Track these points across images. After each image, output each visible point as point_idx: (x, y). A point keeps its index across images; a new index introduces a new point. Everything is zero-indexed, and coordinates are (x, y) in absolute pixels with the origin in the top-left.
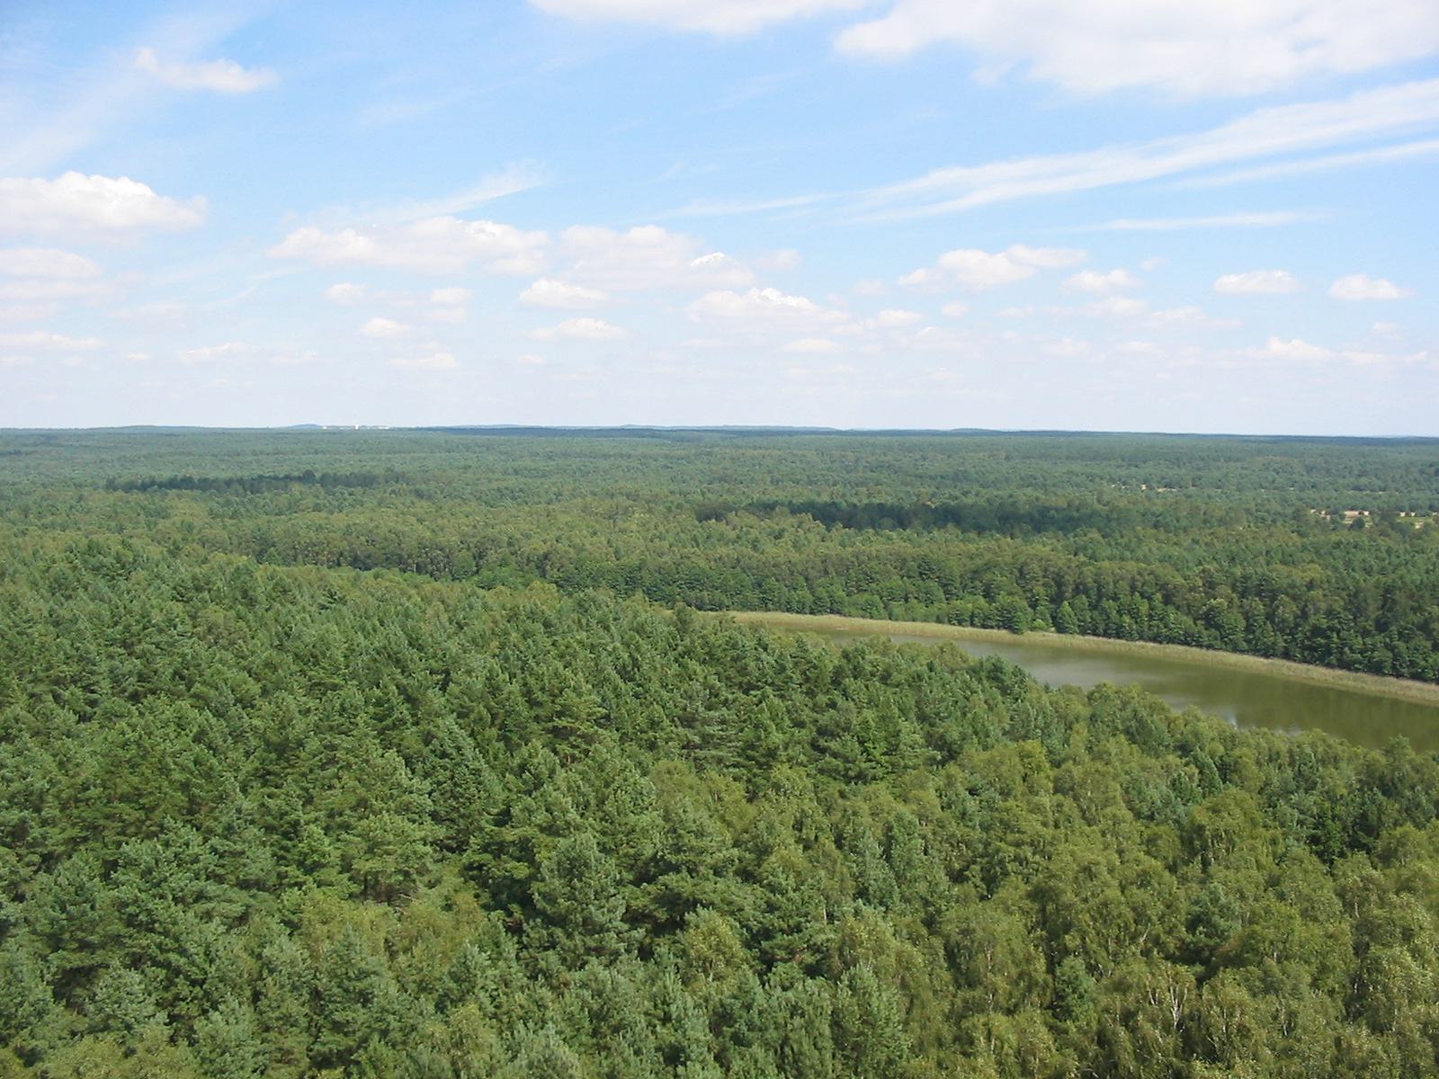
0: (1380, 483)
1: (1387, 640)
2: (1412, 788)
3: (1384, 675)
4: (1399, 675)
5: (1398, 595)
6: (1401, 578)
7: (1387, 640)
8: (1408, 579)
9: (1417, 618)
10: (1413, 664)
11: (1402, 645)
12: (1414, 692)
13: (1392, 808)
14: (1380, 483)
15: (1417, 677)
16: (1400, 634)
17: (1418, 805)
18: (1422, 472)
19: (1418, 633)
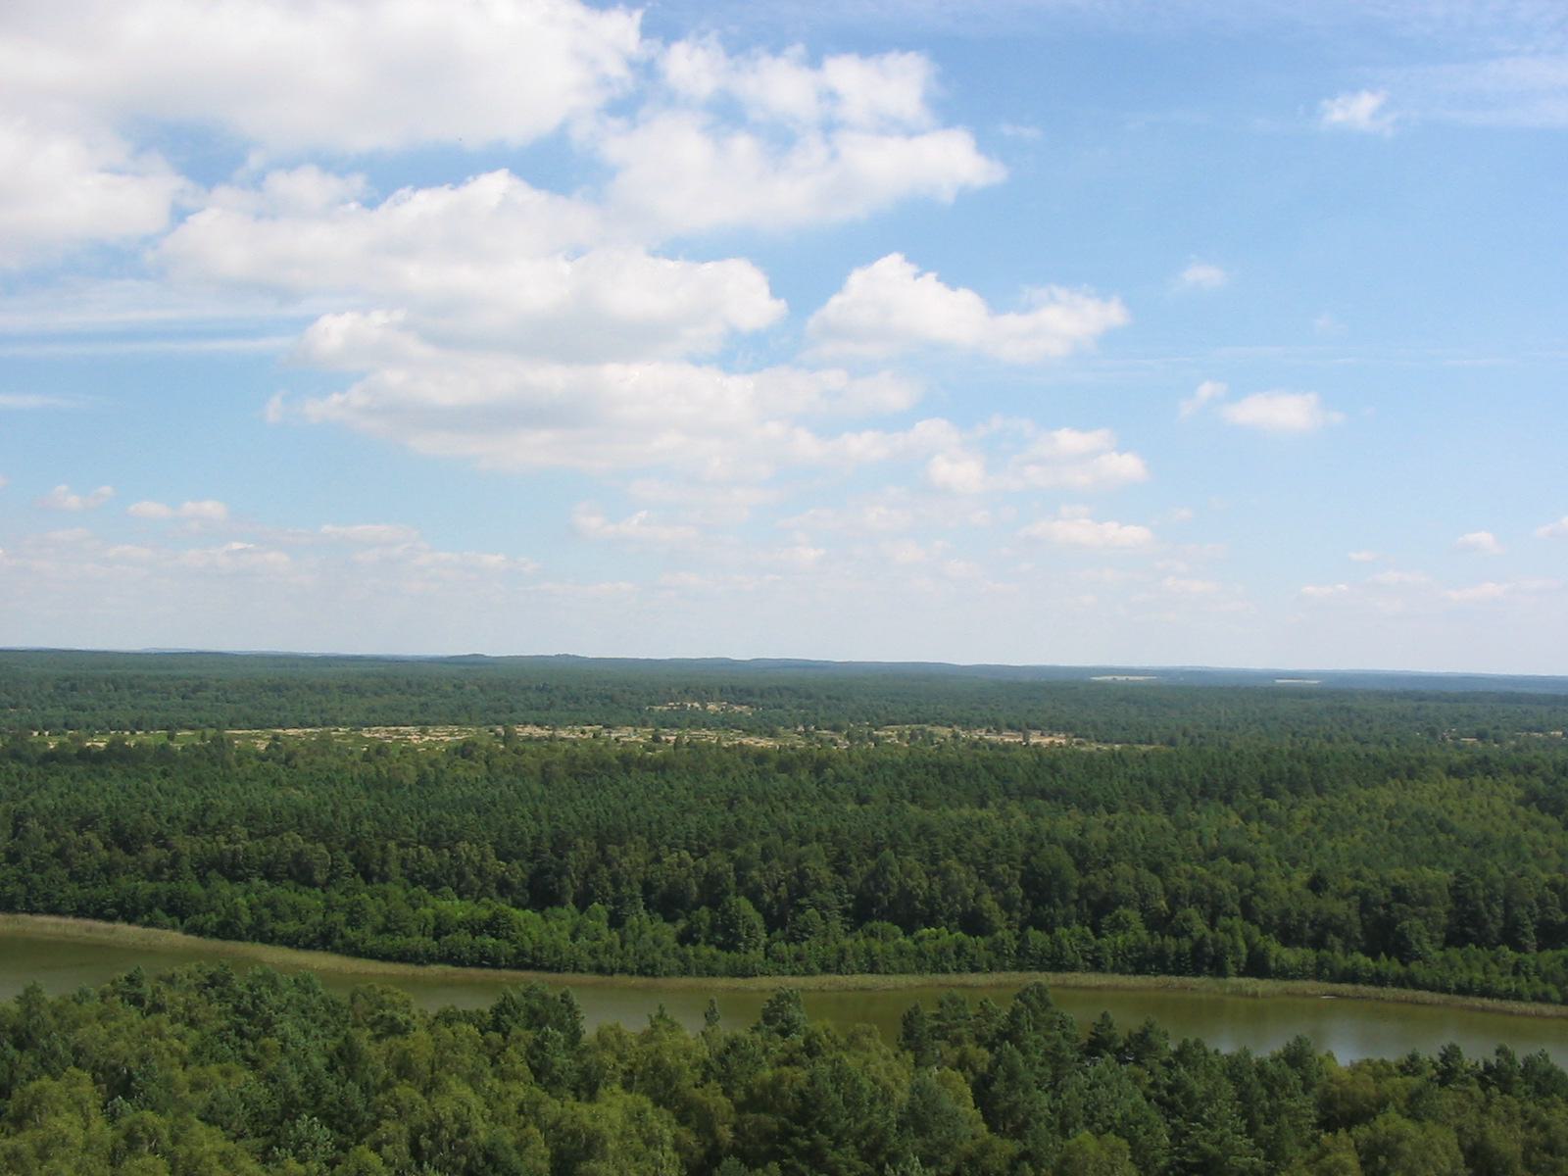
0: (9, 699)
1: (20, 873)
2: (48, 1036)
3: (17, 912)
4: (33, 912)
5: (32, 824)
6: (32, 804)
7: (20, 873)
8: (40, 805)
9: (52, 846)
10: (47, 897)
11: (36, 877)
12: (49, 929)
13: (27, 1060)
14: (9, 699)
15: (54, 911)
16: (33, 863)
17: (54, 1054)
18: (57, 687)
19: (55, 860)
